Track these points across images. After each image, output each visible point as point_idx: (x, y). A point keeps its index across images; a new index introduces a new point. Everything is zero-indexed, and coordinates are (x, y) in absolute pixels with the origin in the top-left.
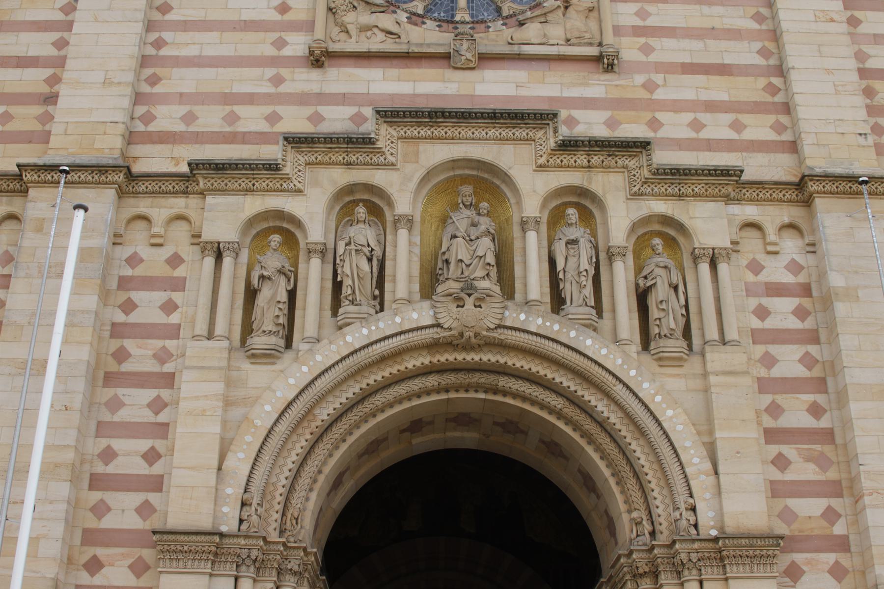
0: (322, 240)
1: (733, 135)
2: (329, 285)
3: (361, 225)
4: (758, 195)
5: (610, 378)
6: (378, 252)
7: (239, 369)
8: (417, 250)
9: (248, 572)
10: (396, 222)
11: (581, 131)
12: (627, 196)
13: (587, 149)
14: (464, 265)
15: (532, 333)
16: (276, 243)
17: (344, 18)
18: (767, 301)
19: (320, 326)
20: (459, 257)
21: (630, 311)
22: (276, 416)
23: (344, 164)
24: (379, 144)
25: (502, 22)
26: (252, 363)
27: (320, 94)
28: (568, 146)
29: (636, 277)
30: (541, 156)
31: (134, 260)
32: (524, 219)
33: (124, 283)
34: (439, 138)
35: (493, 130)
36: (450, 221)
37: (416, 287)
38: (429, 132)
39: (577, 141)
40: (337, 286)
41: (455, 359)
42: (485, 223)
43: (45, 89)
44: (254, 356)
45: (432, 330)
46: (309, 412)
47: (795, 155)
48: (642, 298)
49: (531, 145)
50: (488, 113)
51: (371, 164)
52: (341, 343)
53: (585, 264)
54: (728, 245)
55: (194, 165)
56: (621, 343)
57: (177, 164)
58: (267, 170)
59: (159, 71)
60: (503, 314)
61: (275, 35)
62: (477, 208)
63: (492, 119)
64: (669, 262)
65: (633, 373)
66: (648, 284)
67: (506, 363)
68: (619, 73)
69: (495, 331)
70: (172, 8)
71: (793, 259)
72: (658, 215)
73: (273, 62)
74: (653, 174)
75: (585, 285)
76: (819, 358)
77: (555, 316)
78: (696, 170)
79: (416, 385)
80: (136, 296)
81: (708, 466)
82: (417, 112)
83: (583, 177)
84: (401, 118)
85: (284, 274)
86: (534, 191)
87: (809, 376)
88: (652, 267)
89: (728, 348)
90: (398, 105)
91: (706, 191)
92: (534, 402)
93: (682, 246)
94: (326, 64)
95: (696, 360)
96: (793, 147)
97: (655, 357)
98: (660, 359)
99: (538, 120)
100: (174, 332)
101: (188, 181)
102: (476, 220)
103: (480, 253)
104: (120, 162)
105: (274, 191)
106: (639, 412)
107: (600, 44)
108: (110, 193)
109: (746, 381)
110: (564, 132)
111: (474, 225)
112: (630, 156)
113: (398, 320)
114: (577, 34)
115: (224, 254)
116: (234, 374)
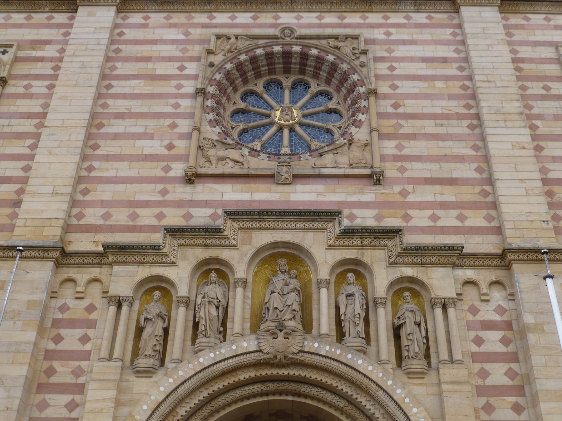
0: (187, 295)
1: (459, 224)
2: (191, 324)
3: (213, 285)
4: (474, 262)
5: (375, 386)
6: (223, 302)
7: (128, 381)
8: (249, 301)
11: (358, 223)
12: (386, 265)
13: (361, 234)
14: (278, 311)
15: (322, 356)
16: (157, 297)
17: (208, 153)
18: (482, 333)
19: (183, 352)
20: (275, 306)
21: (388, 340)
22: (150, 412)
23: (203, 246)
24: (226, 233)
25: (309, 154)
26: (137, 377)
27: (191, 201)
28: (348, 233)
29: (393, 318)
30: (331, 239)
31: (63, 308)
32: (319, 281)
33: (56, 323)
34: (265, 229)
35: (300, 223)
36: (272, 282)
37: (248, 325)
38: (258, 225)
39: (353, 229)
40: (196, 325)
41: (272, 374)
42: (294, 283)
43: (14, 197)
44: (138, 372)
45: (256, 354)
47: (501, 236)
48: (397, 331)
49: (324, 232)
50: (296, 212)
51: (221, 246)
52: (196, 363)
53: (358, 310)
54: (454, 296)
55: (106, 246)
56: (382, 362)
57: (96, 246)
58: (153, 250)
59: (89, 186)
60: (303, 343)
61: (165, 164)
62: (289, 273)
63: (299, 216)
64: (415, 308)
65: (390, 383)
66: (400, 323)
67: (305, 376)
68: (384, 185)
69: (298, 354)
70: (99, 147)
71: (499, 305)
72: (408, 277)
74: (404, 250)
75: (358, 324)
76: (519, 372)
77: (339, 345)
78: (432, 247)
79: (246, 391)
80: (63, 332)
82: (250, 212)
83: (358, 253)
84: (240, 216)
85: (161, 317)
86: (326, 262)
87: (512, 384)
88: (403, 311)
89: (455, 365)
90: (241, 208)
91: (439, 260)
92: (325, 403)
93: (424, 296)
94: (196, 181)
96: (499, 230)
97: (405, 372)
98: (409, 373)
99: (329, 216)
100: (86, 356)
101: (102, 256)
102: (288, 281)
103: (289, 303)
104: (60, 245)
105: (158, 263)
106: (394, 410)
107: (372, 167)
108: (50, 264)
110: (346, 223)
111: (287, 284)
112: (389, 239)
113: (234, 347)
114: (356, 161)
115: (123, 304)
116: (124, 384)
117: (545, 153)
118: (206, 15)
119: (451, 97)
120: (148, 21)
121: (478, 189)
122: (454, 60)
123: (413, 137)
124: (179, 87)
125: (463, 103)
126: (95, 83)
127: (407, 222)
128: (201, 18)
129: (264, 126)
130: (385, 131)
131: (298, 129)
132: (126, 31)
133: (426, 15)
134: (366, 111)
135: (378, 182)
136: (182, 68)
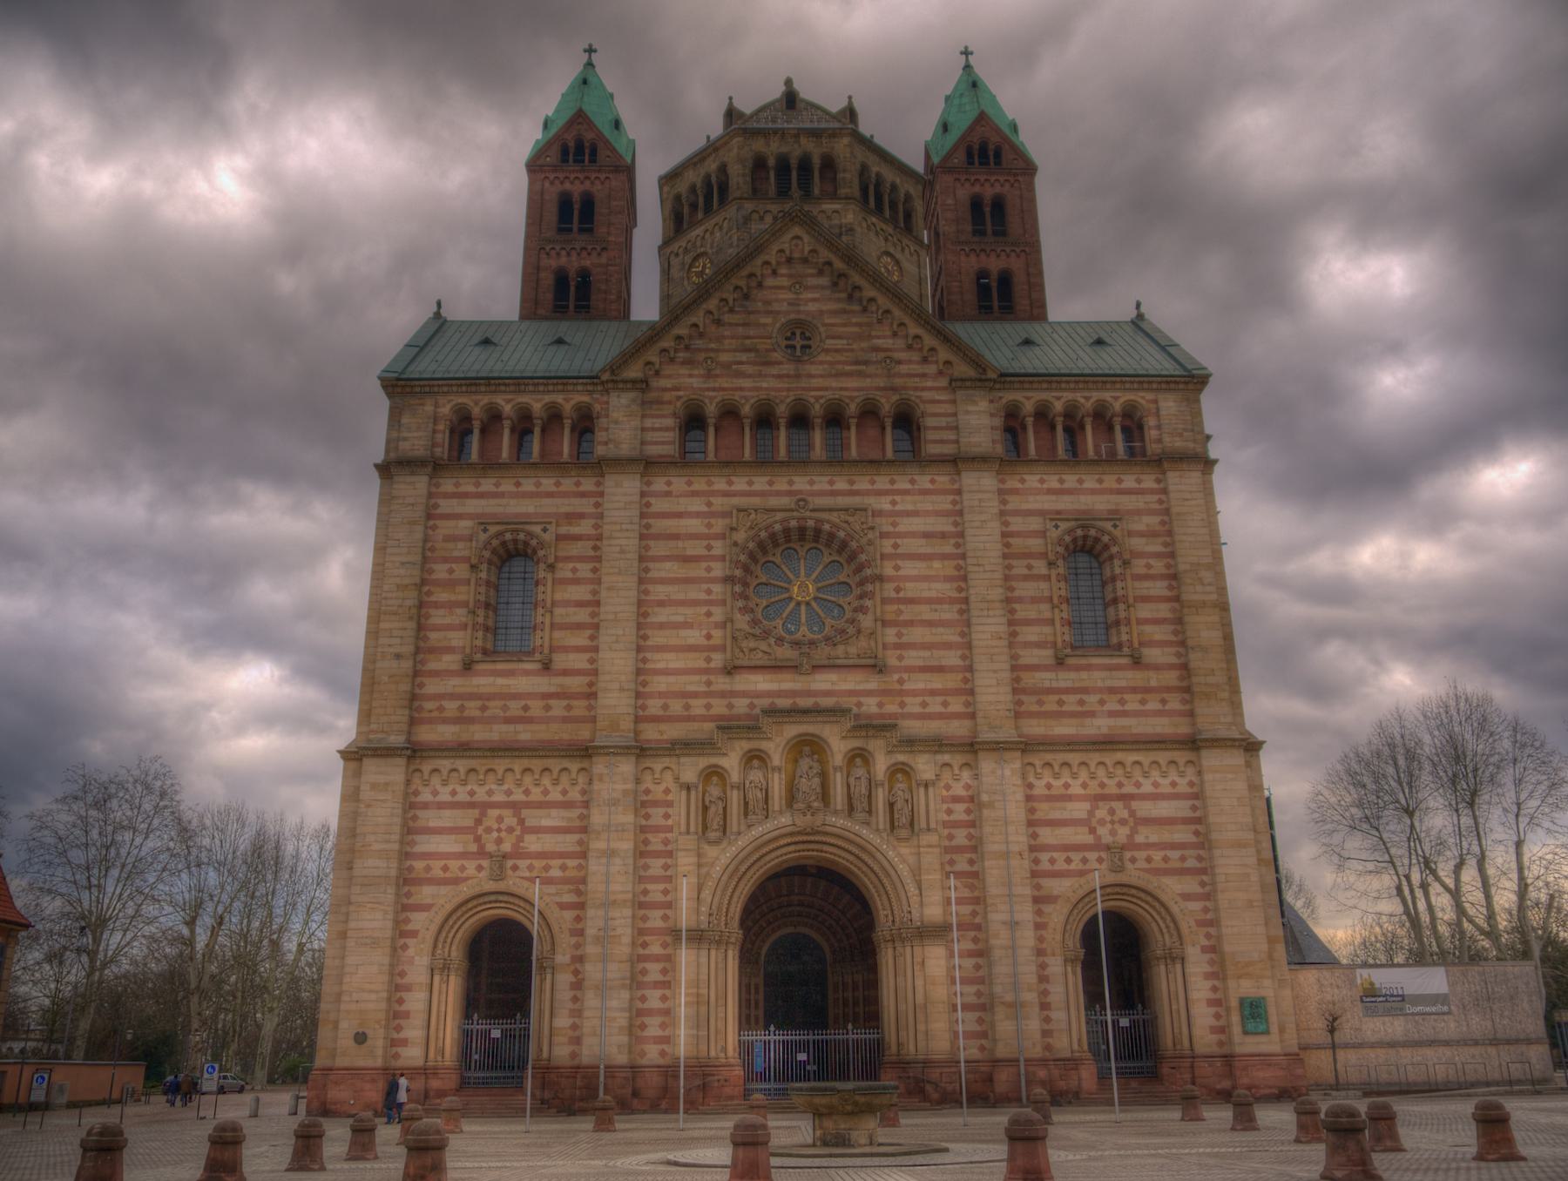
1: (943, 710)
9: (713, 946)
10: (773, 769)
18: (951, 805)
19: (739, 824)
31: (647, 792)
33: (644, 804)
40: (746, 804)
43: (586, 689)
46: (736, 869)
48: (891, 805)
53: (864, 791)
59: (648, 678)
61: (706, 654)
73: (706, 671)
80: (650, 811)
81: (917, 892)
96: (973, 716)
100: (670, 829)
108: (633, 759)
109: (937, 850)
117: (1020, 638)
118: (724, 480)
120: (671, 488)
121: (960, 676)
123: (910, 623)
124: (709, 570)
127: (902, 708)
128: (720, 484)
130: (888, 617)
131: (814, 604)
132: (652, 500)
133: (929, 477)
134: (871, 595)
135: (881, 671)
136: (709, 548)
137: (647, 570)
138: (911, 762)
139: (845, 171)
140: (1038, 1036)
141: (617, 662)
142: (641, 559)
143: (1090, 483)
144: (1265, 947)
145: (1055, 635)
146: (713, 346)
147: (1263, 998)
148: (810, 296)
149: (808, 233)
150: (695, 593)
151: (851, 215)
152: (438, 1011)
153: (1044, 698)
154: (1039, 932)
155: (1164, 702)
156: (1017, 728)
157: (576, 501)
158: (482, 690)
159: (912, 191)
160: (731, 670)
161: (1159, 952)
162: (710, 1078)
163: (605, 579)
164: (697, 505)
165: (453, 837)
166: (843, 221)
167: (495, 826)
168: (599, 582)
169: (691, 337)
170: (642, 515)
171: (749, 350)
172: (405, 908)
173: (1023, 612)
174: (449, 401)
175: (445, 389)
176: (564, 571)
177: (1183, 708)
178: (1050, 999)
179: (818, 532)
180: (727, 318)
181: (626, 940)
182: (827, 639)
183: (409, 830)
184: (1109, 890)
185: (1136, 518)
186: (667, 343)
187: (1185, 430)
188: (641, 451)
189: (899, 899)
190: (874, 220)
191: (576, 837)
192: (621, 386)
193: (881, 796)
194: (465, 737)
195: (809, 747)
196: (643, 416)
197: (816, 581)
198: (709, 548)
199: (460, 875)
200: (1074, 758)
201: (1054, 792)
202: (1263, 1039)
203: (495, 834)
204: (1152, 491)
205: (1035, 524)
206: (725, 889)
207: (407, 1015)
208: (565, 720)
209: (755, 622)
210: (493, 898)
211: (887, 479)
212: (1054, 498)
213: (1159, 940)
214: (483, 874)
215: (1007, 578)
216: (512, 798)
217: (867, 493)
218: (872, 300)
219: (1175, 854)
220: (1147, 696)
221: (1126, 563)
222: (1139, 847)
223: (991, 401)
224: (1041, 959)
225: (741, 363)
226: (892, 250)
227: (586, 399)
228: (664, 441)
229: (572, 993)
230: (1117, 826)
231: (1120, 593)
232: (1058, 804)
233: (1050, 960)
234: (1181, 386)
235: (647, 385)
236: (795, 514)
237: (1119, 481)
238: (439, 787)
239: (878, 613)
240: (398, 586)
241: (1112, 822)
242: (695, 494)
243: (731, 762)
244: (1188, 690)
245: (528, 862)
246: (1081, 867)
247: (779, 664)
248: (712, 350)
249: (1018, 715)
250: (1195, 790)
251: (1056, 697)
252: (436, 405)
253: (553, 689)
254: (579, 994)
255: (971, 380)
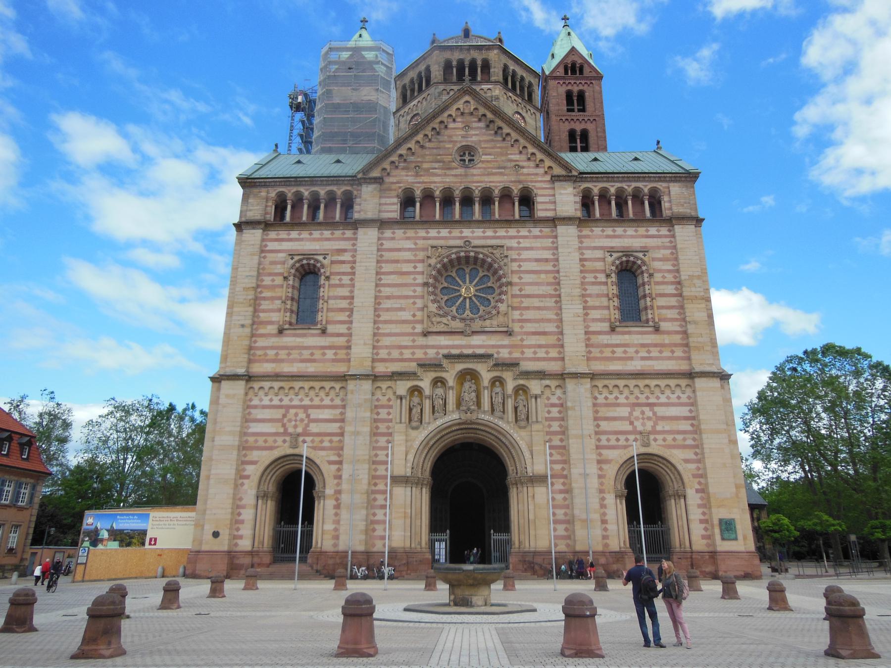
1: (546, 356)
31: (378, 400)
33: (376, 407)
40: (434, 407)
43: (346, 344)
46: (428, 443)
48: (516, 408)
53: (500, 400)
59: (380, 338)
61: (412, 325)
80: (380, 410)
95: (529, 427)
96: (563, 359)
100: (391, 421)
108: (370, 382)
117: (590, 317)
118: (424, 231)
119: (549, 284)
121: (556, 337)
122: (551, 260)
123: (527, 308)
125: (553, 287)
126: (374, 279)
128: (422, 233)
129: (456, 290)
130: (515, 305)
132: (384, 242)
133: (539, 229)
134: (506, 293)
135: (510, 335)
136: (415, 267)
137: (380, 279)
138: (529, 387)
139: (495, 67)
140: (600, 538)
141: (363, 327)
142: (377, 273)
143: (630, 231)
144: (734, 490)
145: (610, 315)
146: (419, 159)
147: (734, 520)
148: (474, 133)
149: (473, 99)
150: (408, 292)
151: (498, 91)
152: (261, 520)
153: (604, 349)
154: (601, 480)
155: (673, 352)
156: (588, 366)
157: (342, 243)
158: (289, 344)
159: (532, 81)
160: (425, 334)
161: (671, 492)
162: (411, 559)
163: (356, 284)
164: (409, 244)
165: (270, 424)
166: (494, 94)
167: (294, 418)
168: (353, 286)
169: (407, 155)
170: (378, 250)
171: (439, 162)
172: (244, 463)
173: (591, 302)
174: (275, 190)
175: (273, 184)
176: (335, 280)
177: (683, 355)
178: (607, 517)
179: (476, 259)
180: (428, 145)
181: (365, 481)
182: (480, 317)
183: (247, 420)
184: (641, 457)
185: (657, 251)
186: (394, 158)
187: (685, 203)
188: (379, 215)
189: (520, 461)
190: (511, 94)
191: (338, 425)
192: (368, 181)
193: (510, 403)
194: (278, 370)
195: (469, 375)
196: (380, 197)
197: (474, 286)
198: (415, 267)
199: (273, 445)
200: (621, 383)
201: (609, 401)
202: (734, 543)
203: (293, 423)
204: (666, 236)
205: (599, 254)
206: (422, 452)
207: (242, 522)
208: (334, 361)
209: (440, 308)
210: (292, 458)
211: (515, 230)
212: (610, 240)
213: (671, 486)
214: (287, 444)
215: (582, 283)
216: (303, 403)
217: (504, 237)
218: (508, 134)
219: (679, 437)
220: (663, 349)
221: (651, 275)
222: (660, 433)
223: (574, 188)
224: (602, 495)
225: (436, 169)
226: (520, 111)
227: (349, 188)
228: (392, 209)
229: (334, 511)
230: (646, 421)
231: (647, 292)
232: (611, 408)
233: (607, 496)
234: (683, 179)
235: (383, 181)
236: (464, 249)
237: (647, 231)
238: (263, 397)
239: (510, 303)
240: (244, 288)
241: (643, 419)
242: (408, 238)
243: (425, 384)
244: (687, 345)
245: (311, 438)
246: (625, 443)
247: (453, 330)
248: (419, 162)
249: (588, 359)
250: (691, 401)
251: (611, 349)
252: (268, 193)
253: (327, 344)
254: (338, 511)
255: (563, 176)
